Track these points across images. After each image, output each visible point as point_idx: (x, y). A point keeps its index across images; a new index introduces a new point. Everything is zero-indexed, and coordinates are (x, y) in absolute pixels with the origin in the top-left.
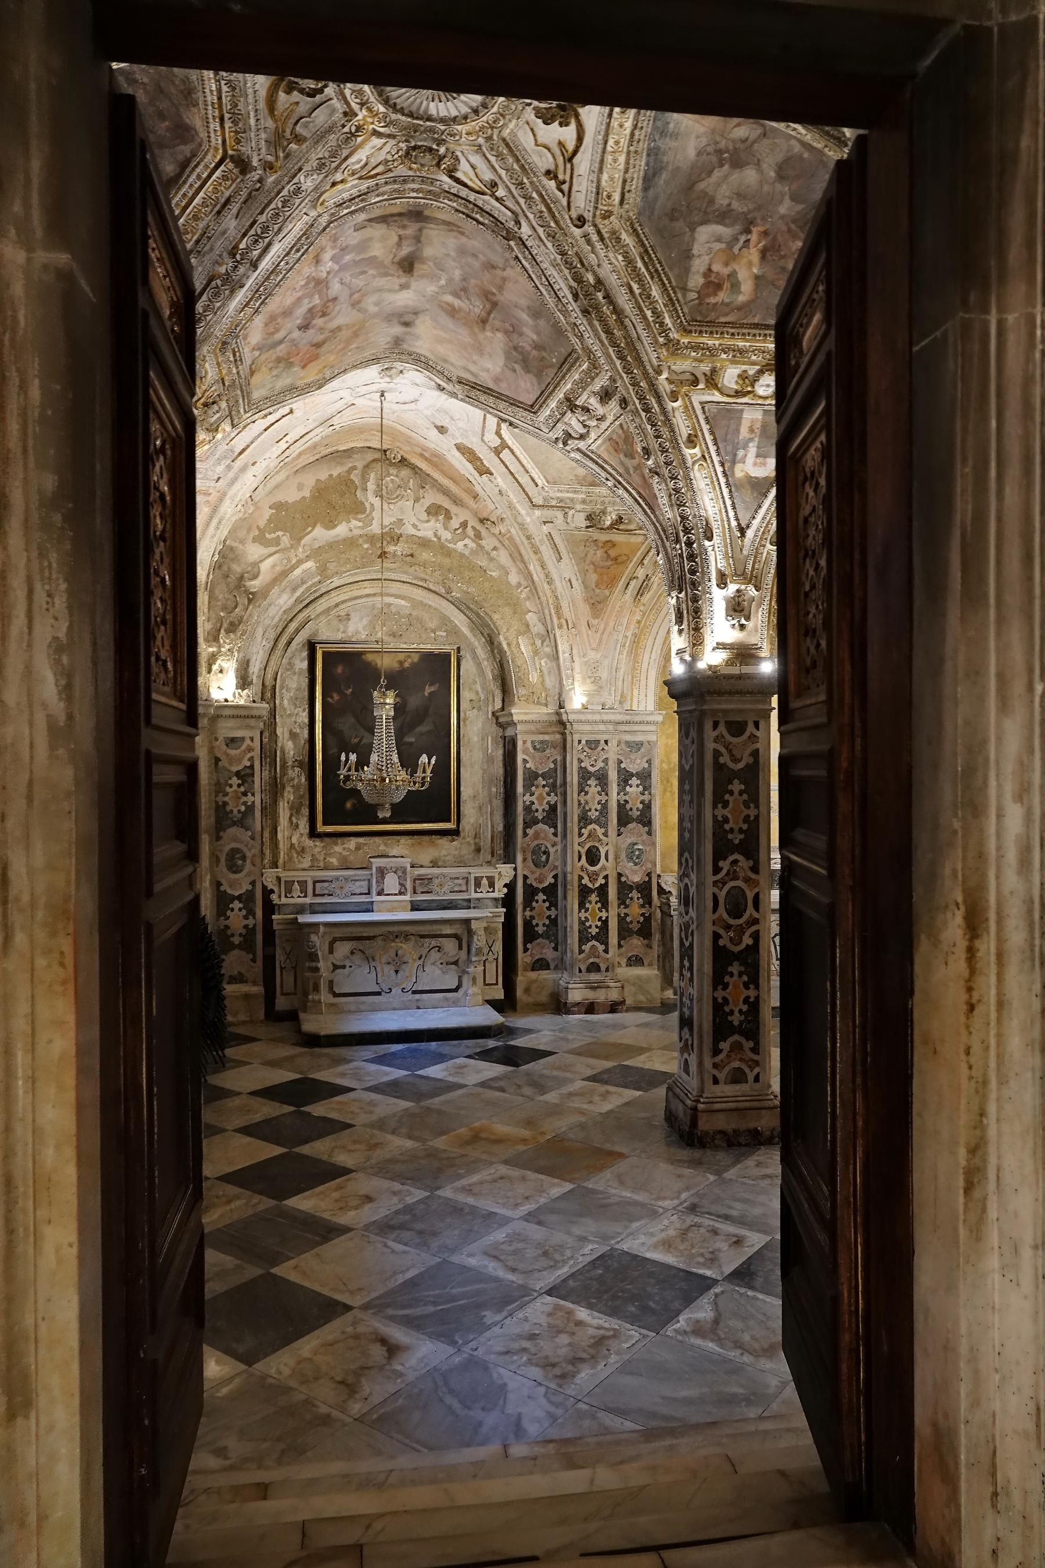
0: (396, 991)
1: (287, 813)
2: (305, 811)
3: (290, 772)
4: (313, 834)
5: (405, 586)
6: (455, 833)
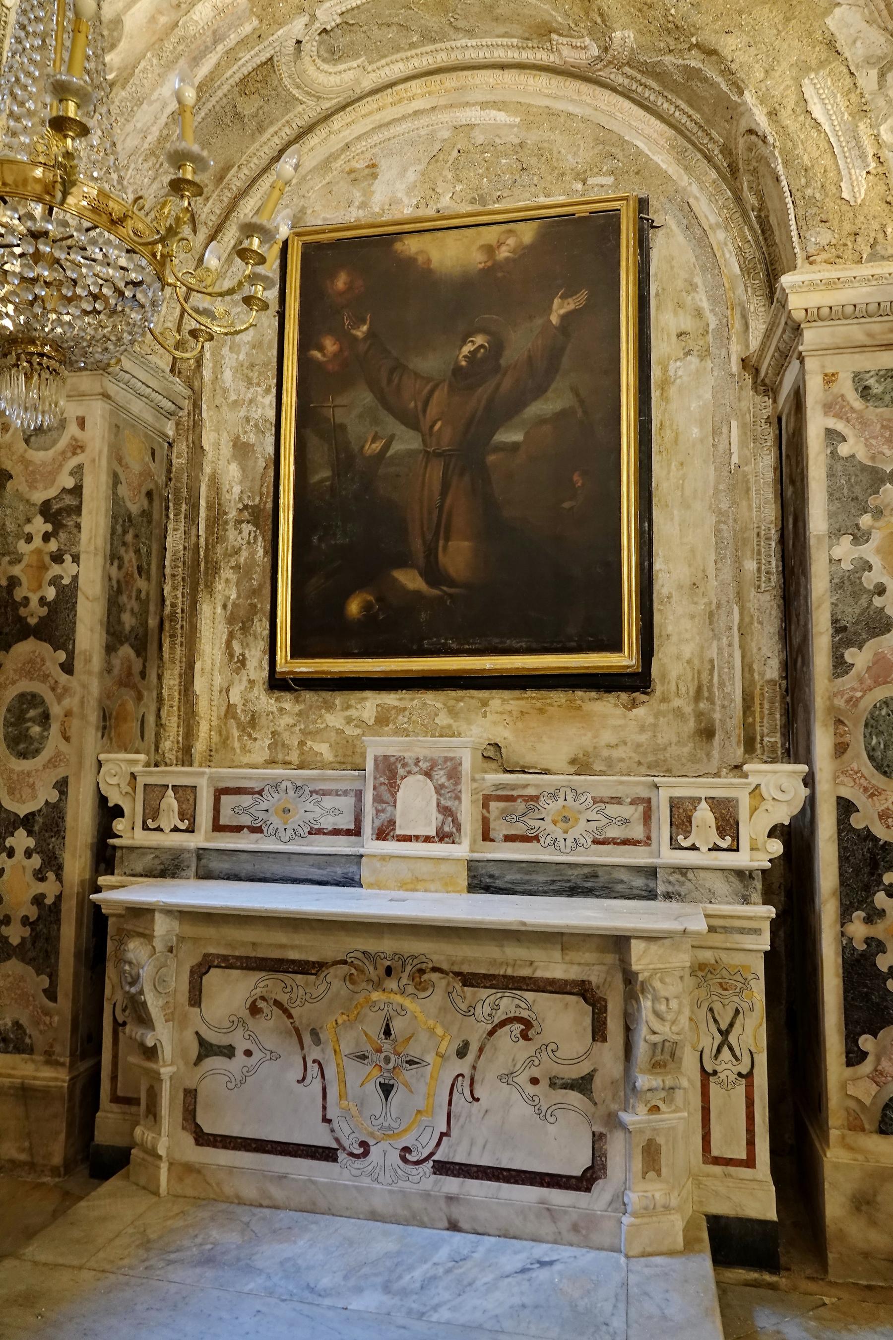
0: (384, 1154)
1: (222, 631)
2: (261, 627)
3: (232, 534)
4: (278, 683)
5: (509, 76)
6: (636, 683)
